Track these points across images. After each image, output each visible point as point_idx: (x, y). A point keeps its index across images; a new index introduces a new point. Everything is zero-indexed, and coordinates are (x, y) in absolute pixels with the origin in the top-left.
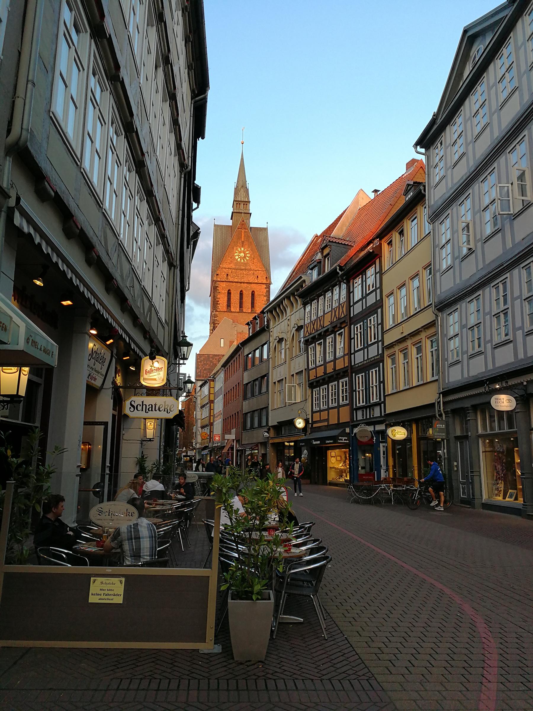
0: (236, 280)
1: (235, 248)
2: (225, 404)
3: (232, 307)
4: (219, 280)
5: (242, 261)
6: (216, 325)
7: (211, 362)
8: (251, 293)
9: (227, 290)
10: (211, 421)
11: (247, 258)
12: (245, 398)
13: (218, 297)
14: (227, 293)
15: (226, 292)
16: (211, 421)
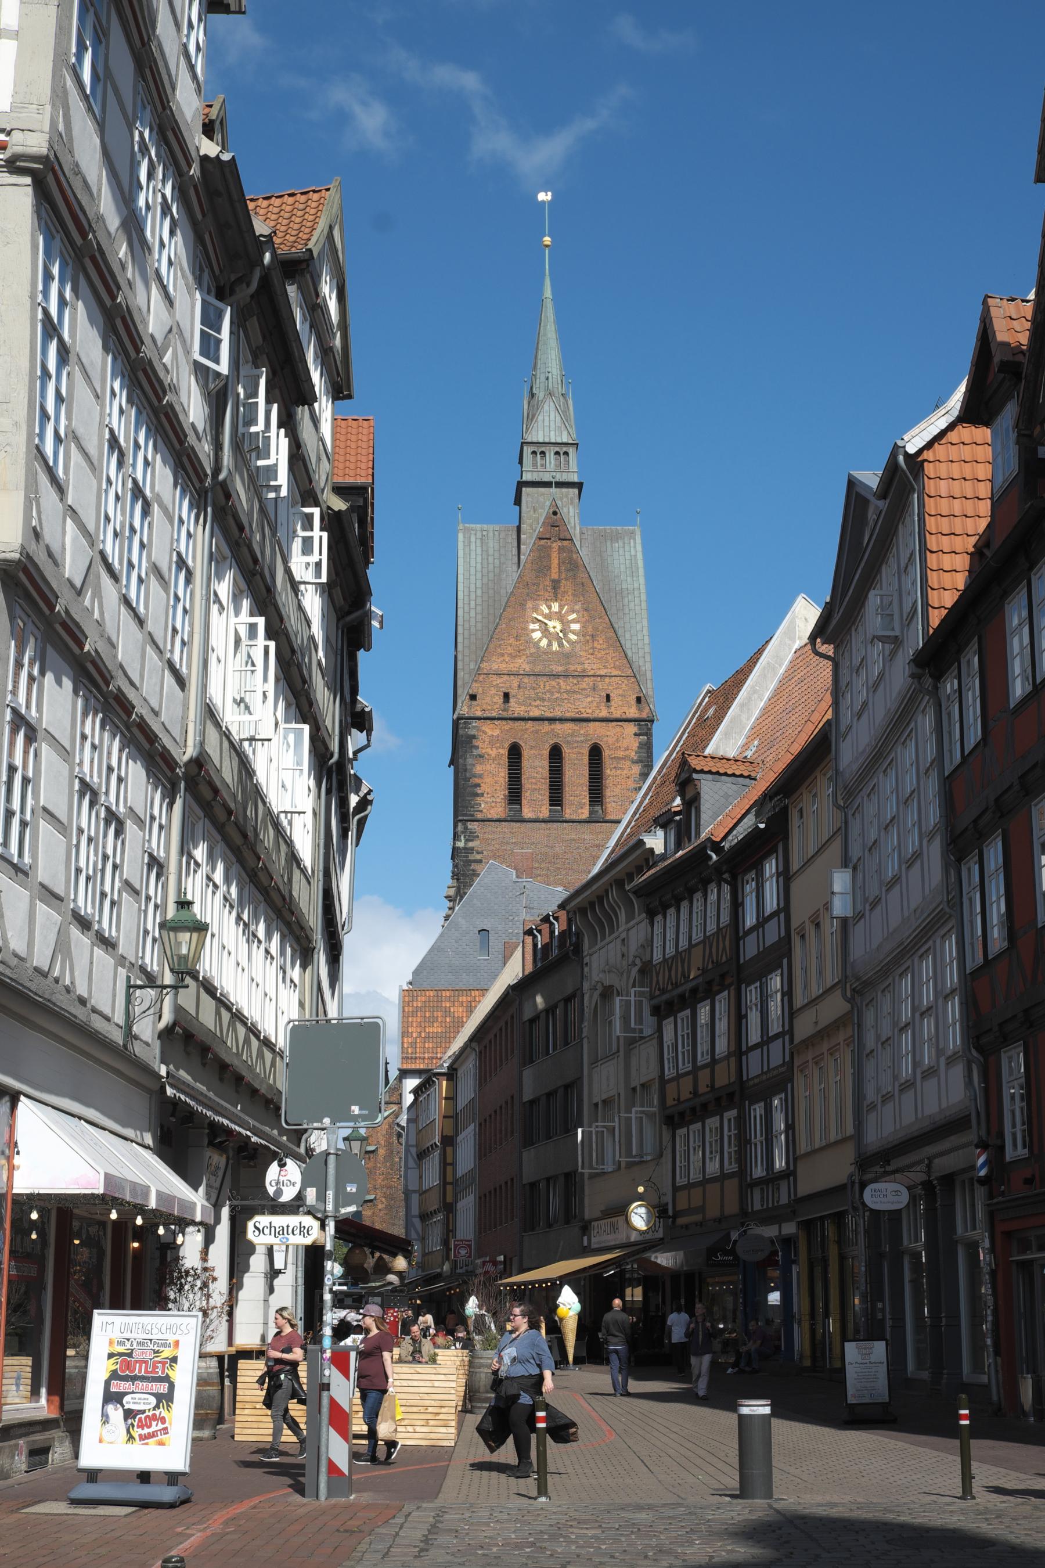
0: (536, 713)
1: (530, 604)
2: (483, 1150)
3: (524, 802)
4: (479, 714)
5: (555, 646)
6: (474, 866)
7: (447, 1012)
8: (586, 752)
9: (507, 745)
10: (449, 1199)
11: (573, 637)
12: (528, 1141)
13: (478, 769)
14: (505, 760)
15: (505, 752)
16: (449, 1199)
